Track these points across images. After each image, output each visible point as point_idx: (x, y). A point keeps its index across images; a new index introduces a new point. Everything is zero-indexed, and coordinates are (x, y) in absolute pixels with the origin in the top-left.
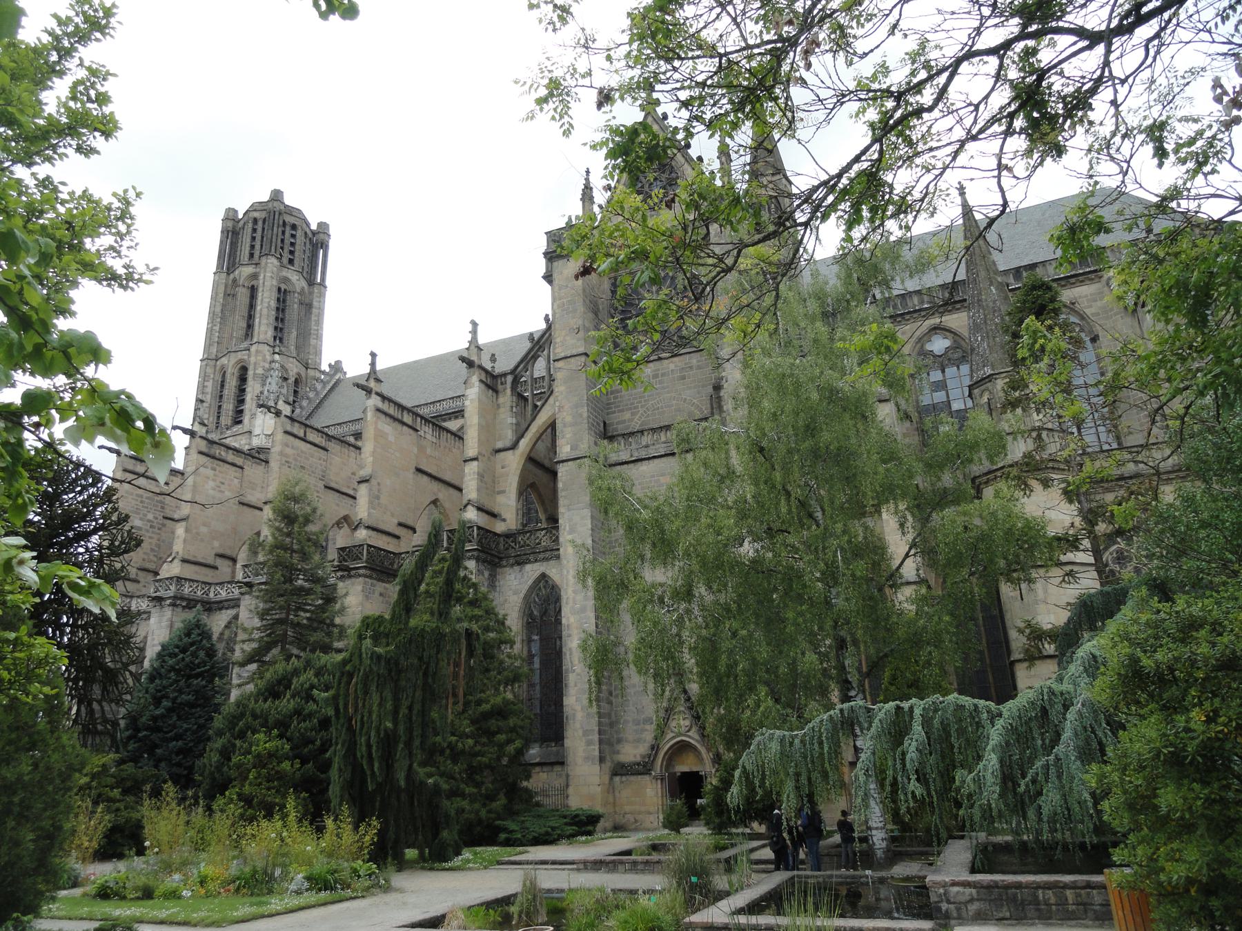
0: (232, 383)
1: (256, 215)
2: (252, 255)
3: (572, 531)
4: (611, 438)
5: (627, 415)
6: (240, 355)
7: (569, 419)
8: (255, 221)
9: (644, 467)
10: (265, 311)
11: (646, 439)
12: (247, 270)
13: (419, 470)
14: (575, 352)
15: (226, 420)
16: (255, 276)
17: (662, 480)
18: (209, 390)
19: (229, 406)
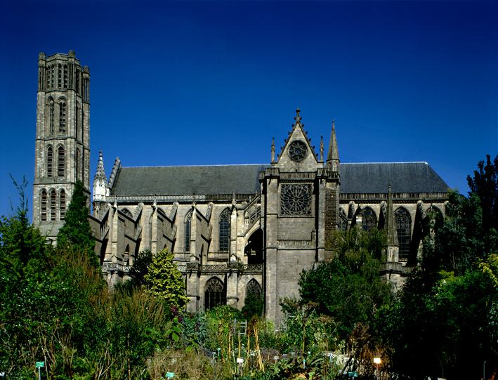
0: (56, 156)
1: (60, 62)
2: (60, 86)
3: (270, 270)
4: (280, 241)
5: (284, 234)
6: (59, 142)
7: (271, 235)
8: (60, 66)
9: (290, 252)
10: (73, 121)
11: (290, 243)
12: (59, 94)
13: (202, 236)
14: (272, 212)
15: (55, 173)
16: (62, 98)
17: (296, 257)
18: (43, 156)
19: (55, 167)
